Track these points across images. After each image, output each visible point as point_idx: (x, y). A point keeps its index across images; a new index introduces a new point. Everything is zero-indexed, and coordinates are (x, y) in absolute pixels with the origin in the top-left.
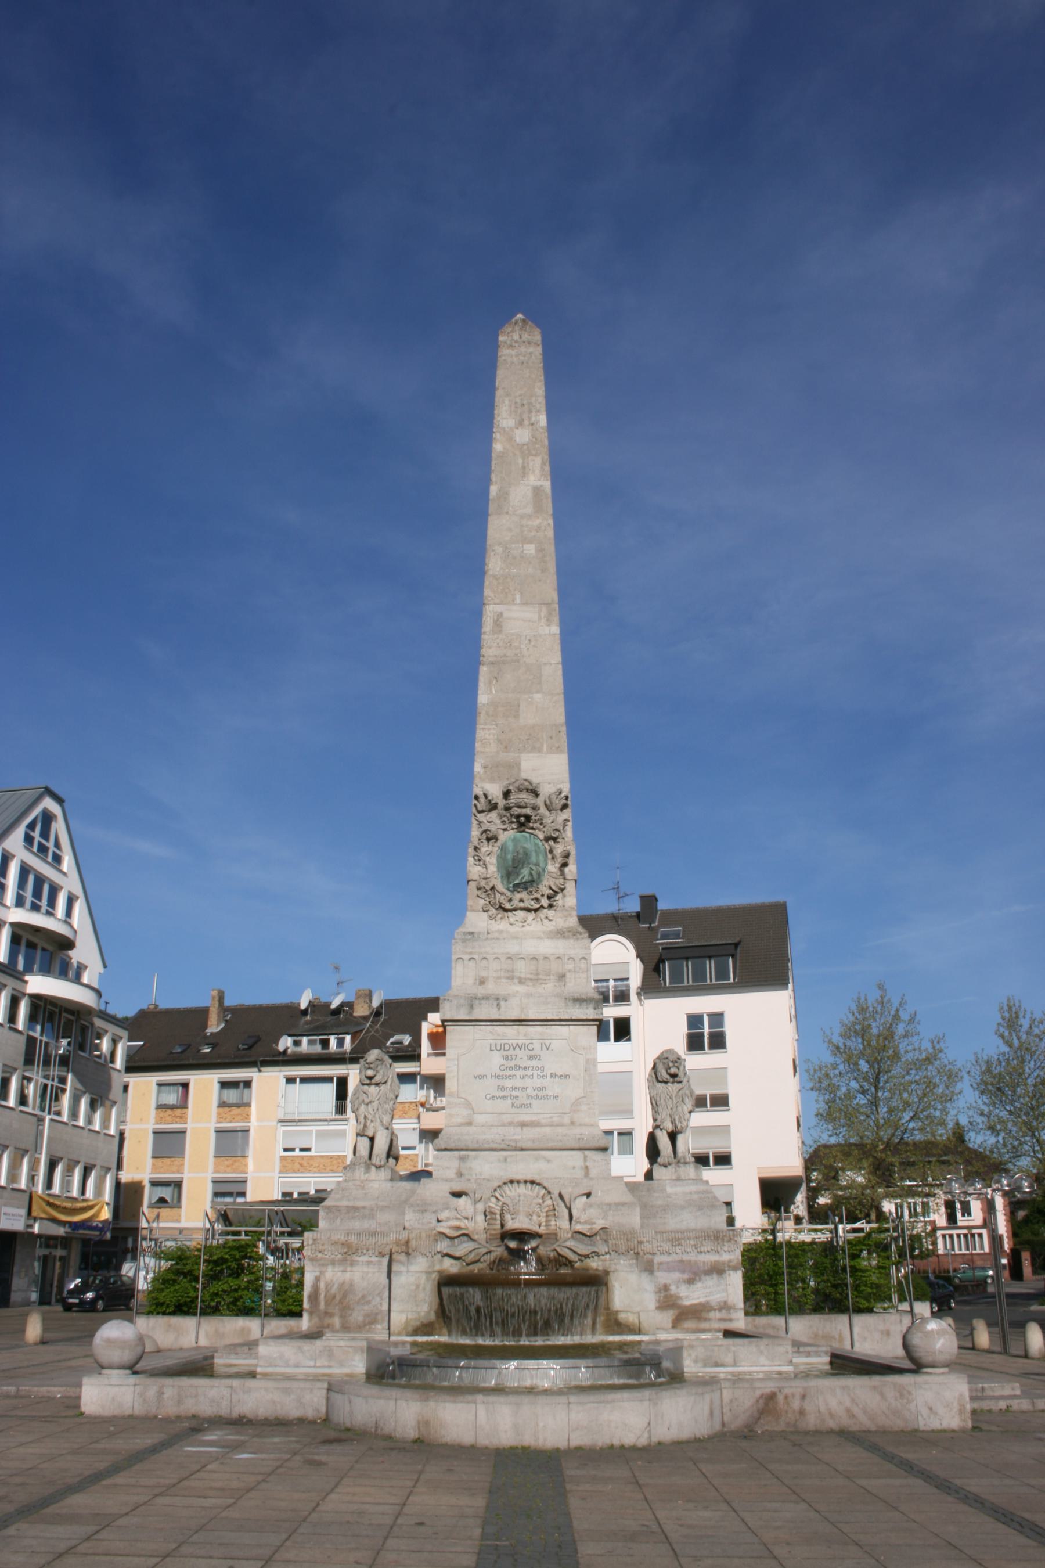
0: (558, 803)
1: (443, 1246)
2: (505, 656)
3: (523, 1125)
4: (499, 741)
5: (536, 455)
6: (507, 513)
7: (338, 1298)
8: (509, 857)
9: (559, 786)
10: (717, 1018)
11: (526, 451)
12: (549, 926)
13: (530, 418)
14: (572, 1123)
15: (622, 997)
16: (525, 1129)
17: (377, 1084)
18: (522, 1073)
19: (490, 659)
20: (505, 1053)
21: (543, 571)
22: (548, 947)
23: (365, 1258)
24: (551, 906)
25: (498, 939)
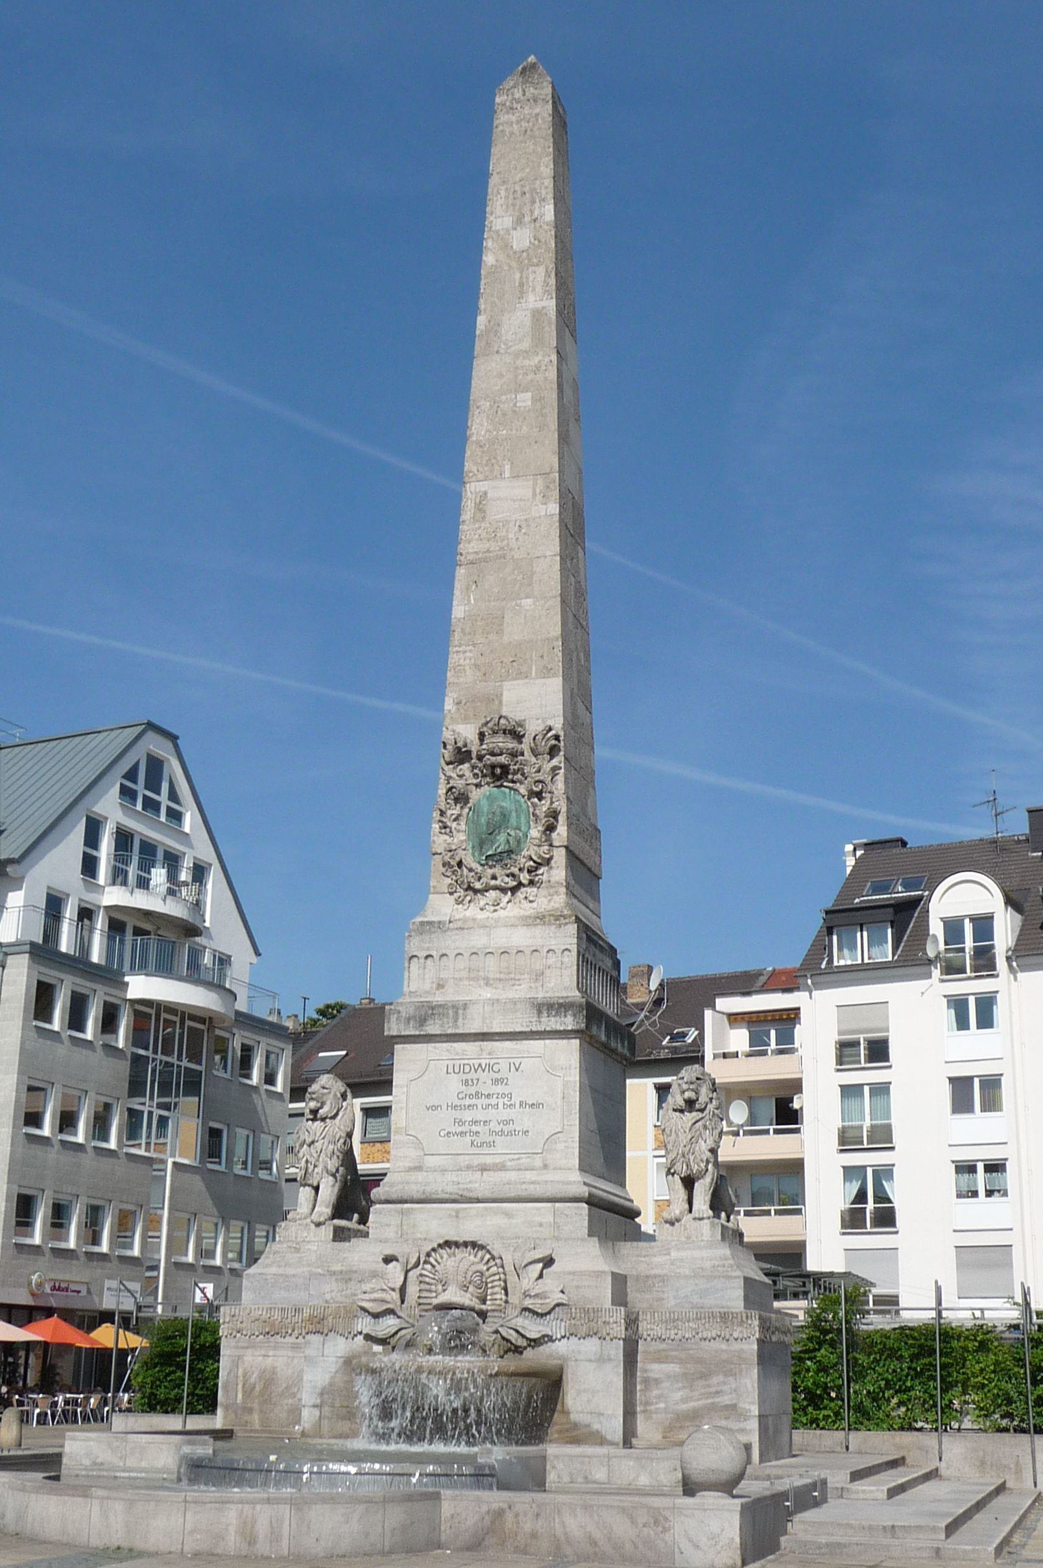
0: (544, 746)
1: (365, 1324)
3: (484, 1169)
7: (257, 1389)
8: (483, 820)
9: (550, 723)
11: (523, 260)
12: (528, 909)
13: (532, 212)
14: (545, 1166)
16: (485, 1173)
17: (323, 1119)
18: (487, 1101)
19: (470, 557)
20: (465, 1077)
21: (541, 429)
22: (522, 938)
25: (462, 929)
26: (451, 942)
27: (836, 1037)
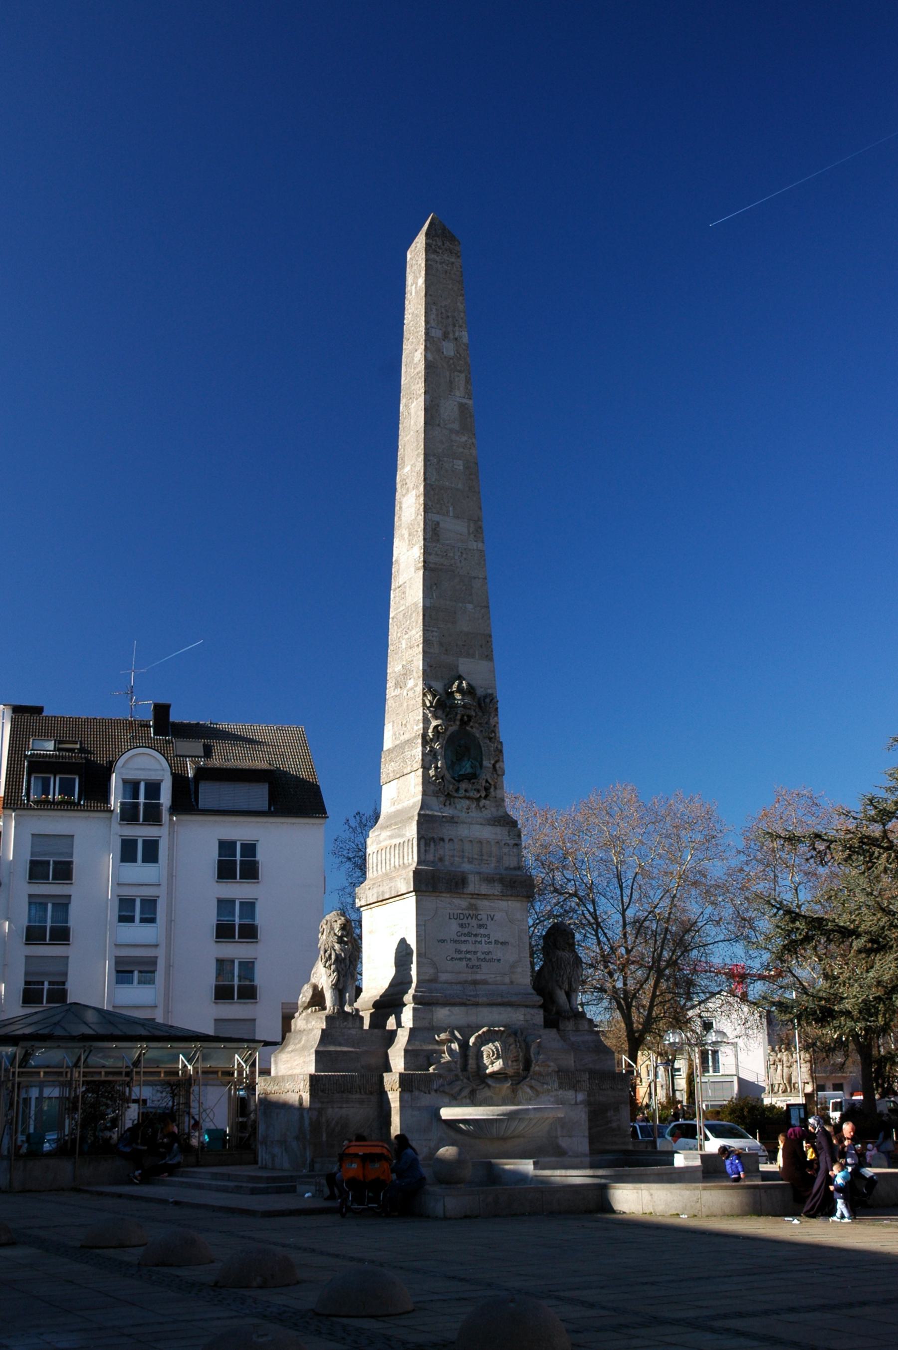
2: (442, 564)
4: (441, 644)
5: (460, 371)
6: (439, 425)
10: (250, 849)
12: (487, 814)
13: (454, 332)
14: (512, 982)
15: (153, 816)
16: (477, 986)
18: (473, 939)
19: (431, 565)
20: (461, 922)
23: (358, 1096)
24: (486, 797)
26: (447, 831)
27: (28, 858)
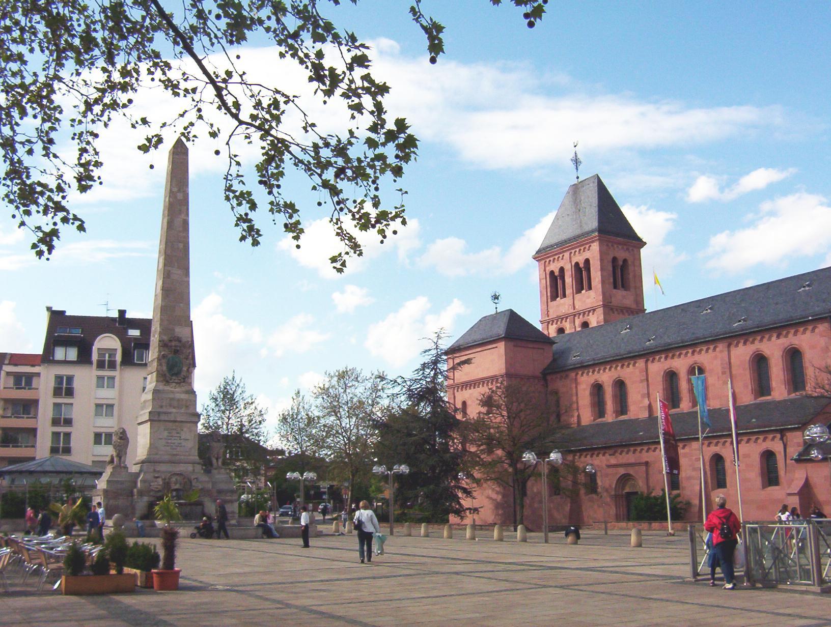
12: (183, 389)
15: (112, 365)
